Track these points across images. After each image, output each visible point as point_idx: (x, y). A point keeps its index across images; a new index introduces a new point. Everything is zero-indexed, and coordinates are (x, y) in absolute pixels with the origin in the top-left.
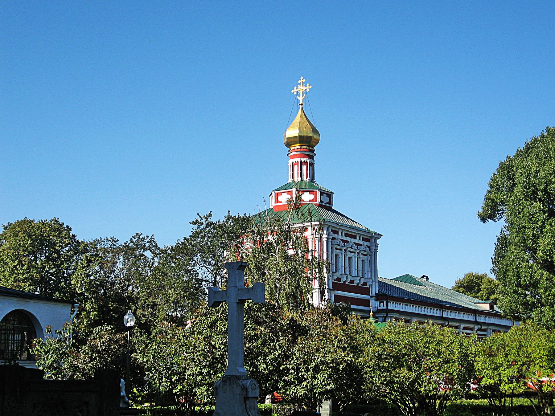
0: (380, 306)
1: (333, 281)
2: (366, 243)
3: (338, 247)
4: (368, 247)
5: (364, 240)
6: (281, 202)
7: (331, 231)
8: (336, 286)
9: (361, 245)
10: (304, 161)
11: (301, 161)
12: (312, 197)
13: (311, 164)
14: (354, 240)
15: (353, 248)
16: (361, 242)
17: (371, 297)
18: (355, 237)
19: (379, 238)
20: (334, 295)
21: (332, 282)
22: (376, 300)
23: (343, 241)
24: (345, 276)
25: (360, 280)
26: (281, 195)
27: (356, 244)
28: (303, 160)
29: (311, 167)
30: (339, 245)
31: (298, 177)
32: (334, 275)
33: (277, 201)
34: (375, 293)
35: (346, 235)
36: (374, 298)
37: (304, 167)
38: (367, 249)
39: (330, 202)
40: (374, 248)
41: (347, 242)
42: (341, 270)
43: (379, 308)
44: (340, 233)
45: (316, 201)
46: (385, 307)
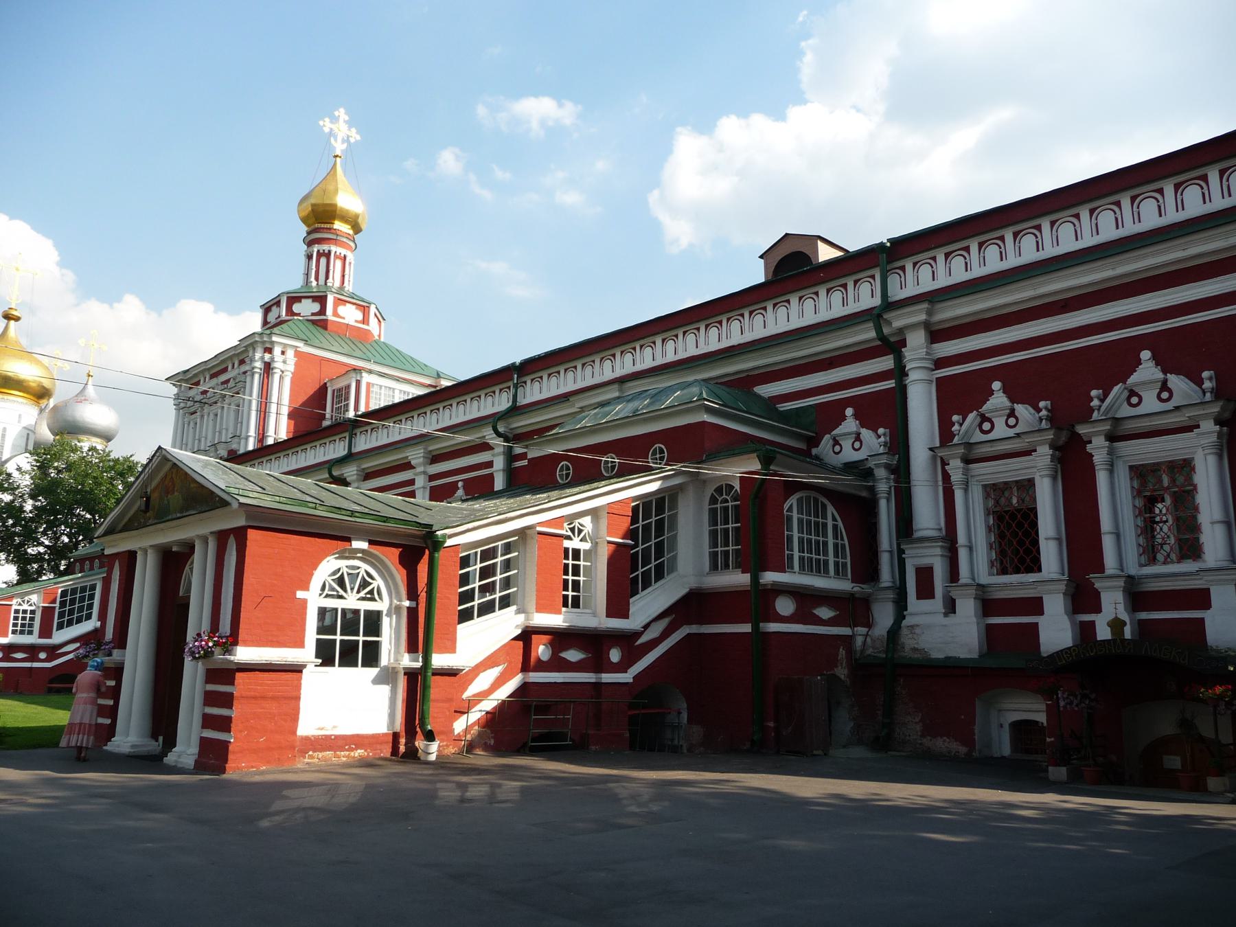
29: (339, 263)
37: (323, 261)
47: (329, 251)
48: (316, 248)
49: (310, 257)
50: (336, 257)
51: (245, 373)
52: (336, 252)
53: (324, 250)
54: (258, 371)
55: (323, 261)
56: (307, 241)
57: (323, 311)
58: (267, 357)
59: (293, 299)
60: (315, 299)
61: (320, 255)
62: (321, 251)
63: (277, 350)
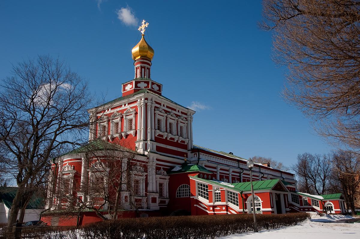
1: (156, 136)
4: (186, 118)
6: (127, 90)
8: (158, 139)
10: (143, 66)
12: (146, 85)
13: (149, 69)
16: (180, 114)
17: (188, 151)
18: (175, 110)
20: (156, 146)
21: (155, 137)
23: (164, 110)
26: (127, 86)
27: (175, 114)
29: (148, 70)
33: (124, 90)
35: (167, 107)
36: (190, 151)
39: (160, 90)
47: (145, 66)
50: (147, 68)
51: (136, 107)
53: (143, 66)
55: (143, 69)
57: (148, 86)
60: (145, 82)
61: (142, 67)
62: (142, 66)
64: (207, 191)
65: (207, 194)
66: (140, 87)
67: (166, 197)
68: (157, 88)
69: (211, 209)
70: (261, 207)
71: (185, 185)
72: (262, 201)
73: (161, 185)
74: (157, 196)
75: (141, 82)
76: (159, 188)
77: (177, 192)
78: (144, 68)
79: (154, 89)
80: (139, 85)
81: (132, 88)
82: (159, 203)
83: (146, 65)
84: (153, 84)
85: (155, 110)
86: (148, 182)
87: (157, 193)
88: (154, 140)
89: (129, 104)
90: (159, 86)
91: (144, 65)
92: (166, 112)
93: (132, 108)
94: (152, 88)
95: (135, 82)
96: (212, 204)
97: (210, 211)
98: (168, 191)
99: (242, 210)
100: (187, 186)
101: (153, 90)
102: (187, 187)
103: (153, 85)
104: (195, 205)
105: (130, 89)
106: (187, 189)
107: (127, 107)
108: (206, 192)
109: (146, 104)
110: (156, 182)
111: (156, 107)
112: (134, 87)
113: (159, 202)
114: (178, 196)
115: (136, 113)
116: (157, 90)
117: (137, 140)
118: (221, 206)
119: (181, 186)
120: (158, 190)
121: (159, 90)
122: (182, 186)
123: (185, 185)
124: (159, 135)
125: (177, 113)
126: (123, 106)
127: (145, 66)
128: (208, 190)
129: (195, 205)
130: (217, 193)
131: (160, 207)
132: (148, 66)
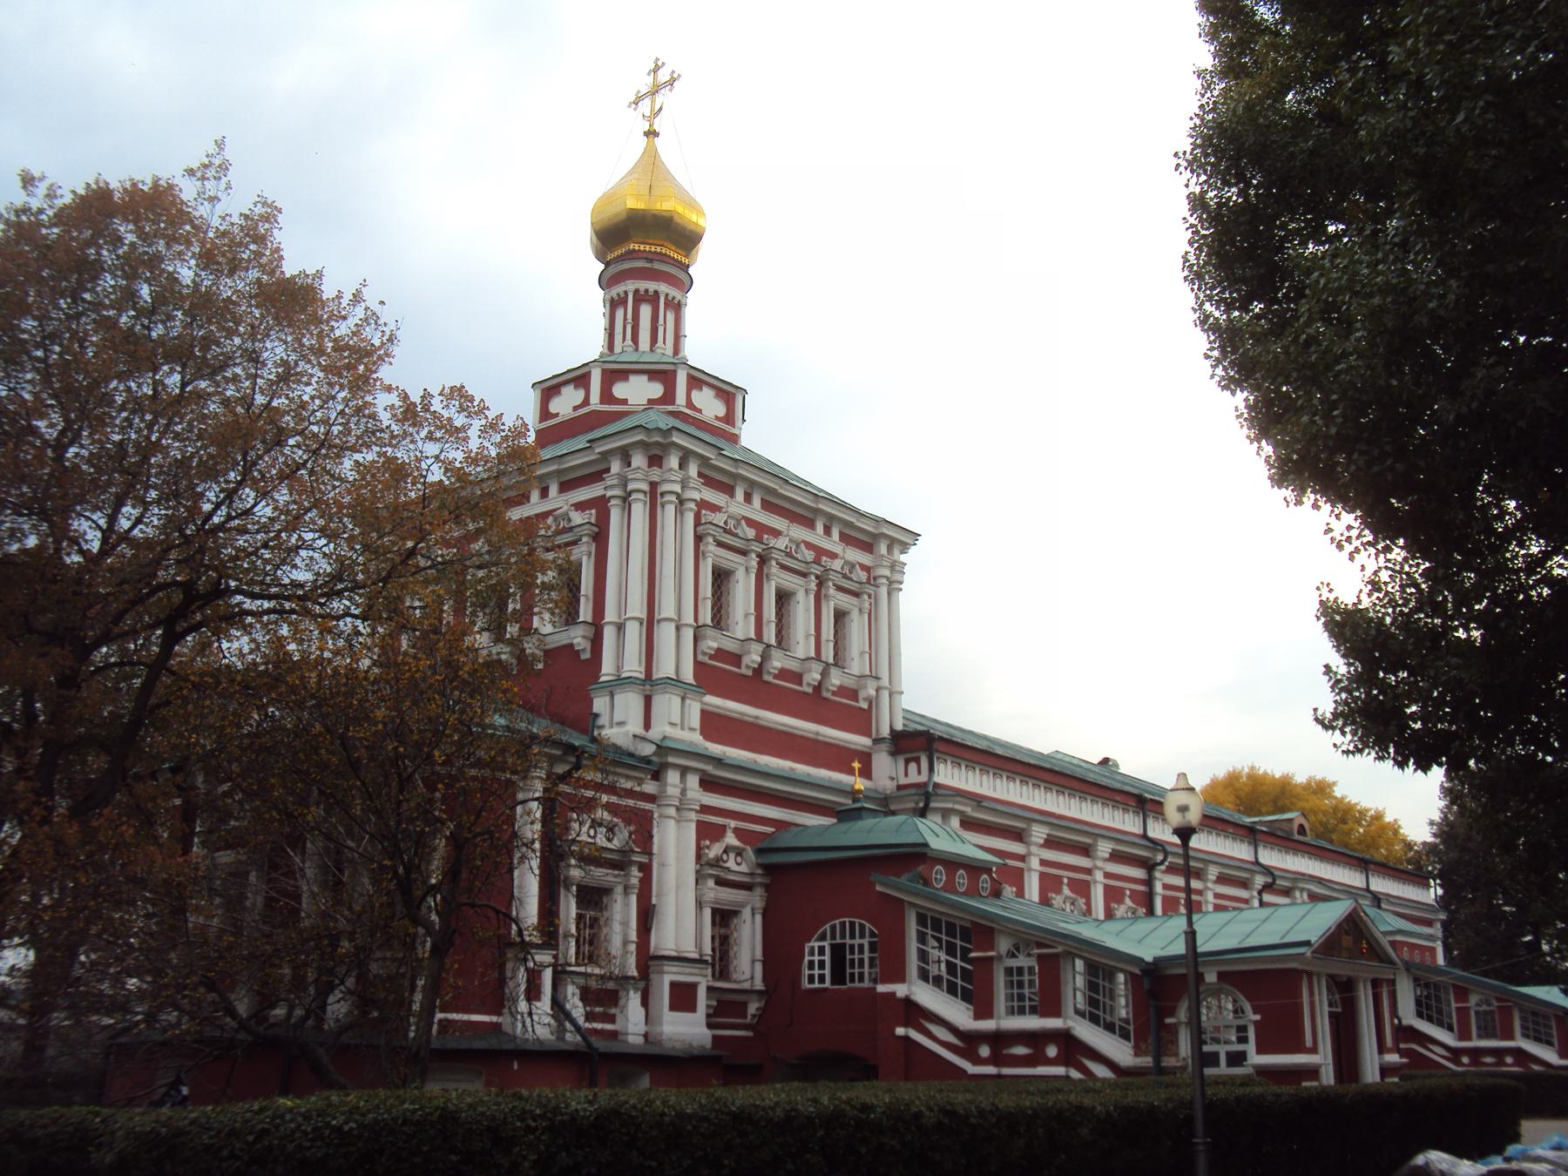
0: (906, 775)
1: (700, 658)
2: (854, 555)
3: (727, 539)
5: (846, 539)
6: (557, 415)
7: (693, 470)
9: (833, 556)
10: (647, 291)
11: (637, 291)
12: (657, 390)
13: (677, 307)
14: (799, 532)
15: (797, 559)
16: (833, 544)
18: (809, 523)
19: (905, 547)
20: (703, 712)
21: (698, 664)
22: (894, 753)
23: (751, 523)
24: (759, 648)
25: (825, 674)
26: (559, 393)
27: (809, 546)
28: (643, 285)
29: (671, 317)
30: (736, 535)
31: (624, 340)
32: (705, 637)
34: (892, 729)
35: (767, 506)
37: (646, 311)
38: (863, 576)
39: (729, 418)
40: (887, 572)
41: (776, 533)
42: (741, 626)
43: (903, 781)
44: (740, 494)
45: (673, 402)
46: (924, 778)
47: (656, 292)
48: (630, 286)
49: (614, 304)
51: (601, 505)
52: (667, 295)
53: (647, 291)
54: (641, 496)
55: (646, 311)
56: (604, 280)
57: (669, 397)
58: (655, 474)
59: (614, 375)
60: (654, 375)
63: (673, 462)
64: (964, 958)
65: (966, 976)
66: (624, 402)
67: (746, 986)
68: (719, 409)
69: (985, 1051)
70: (1251, 1047)
71: (852, 924)
72: (1258, 1017)
73: (724, 918)
74: (703, 981)
75: (632, 378)
76: (713, 938)
77: (807, 958)
78: (653, 299)
79: (700, 411)
80: (619, 390)
81: (586, 402)
82: (708, 1016)
83: (663, 288)
84: (698, 380)
85: (697, 523)
86: (654, 901)
87: (700, 961)
88: (693, 682)
89: (565, 487)
90: (729, 394)
91: (652, 286)
92: (761, 529)
93: (580, 506)
94: (690, 404)
95: (604, 372)
96: (988, 1025)
97: (978, 1061)
98: (759, 953)
99: (1146, 1061)
100: (862, 927)
101: (697, 415)
102: (862, 936)
103: (695, 394)
104: (900, 1031)
105: (575, 408)
106: (861, 947)
107: (558, 501)
108: (958, 962)
109: (653, 485)
110: (700, 905)
111: (703, 504)
112: (595, 397)
113: (708, 1006)
114: (811, 979)
115: (600, 538)
116: (717, 418)
117: (602, 679)
118: (1036, 1039)
119: (827, 926)
120: (708, 950)
121: (727, 413)
122: (833, 928)
123: (852, 924)
124: (720, 654)
125: (817, 537)
126: (535, 496)
127: (656, 292)
128: (970, 951)
129: (900, 1031)
130: (1020, 970)
131: (714, 1037)
132: (674, 292)
